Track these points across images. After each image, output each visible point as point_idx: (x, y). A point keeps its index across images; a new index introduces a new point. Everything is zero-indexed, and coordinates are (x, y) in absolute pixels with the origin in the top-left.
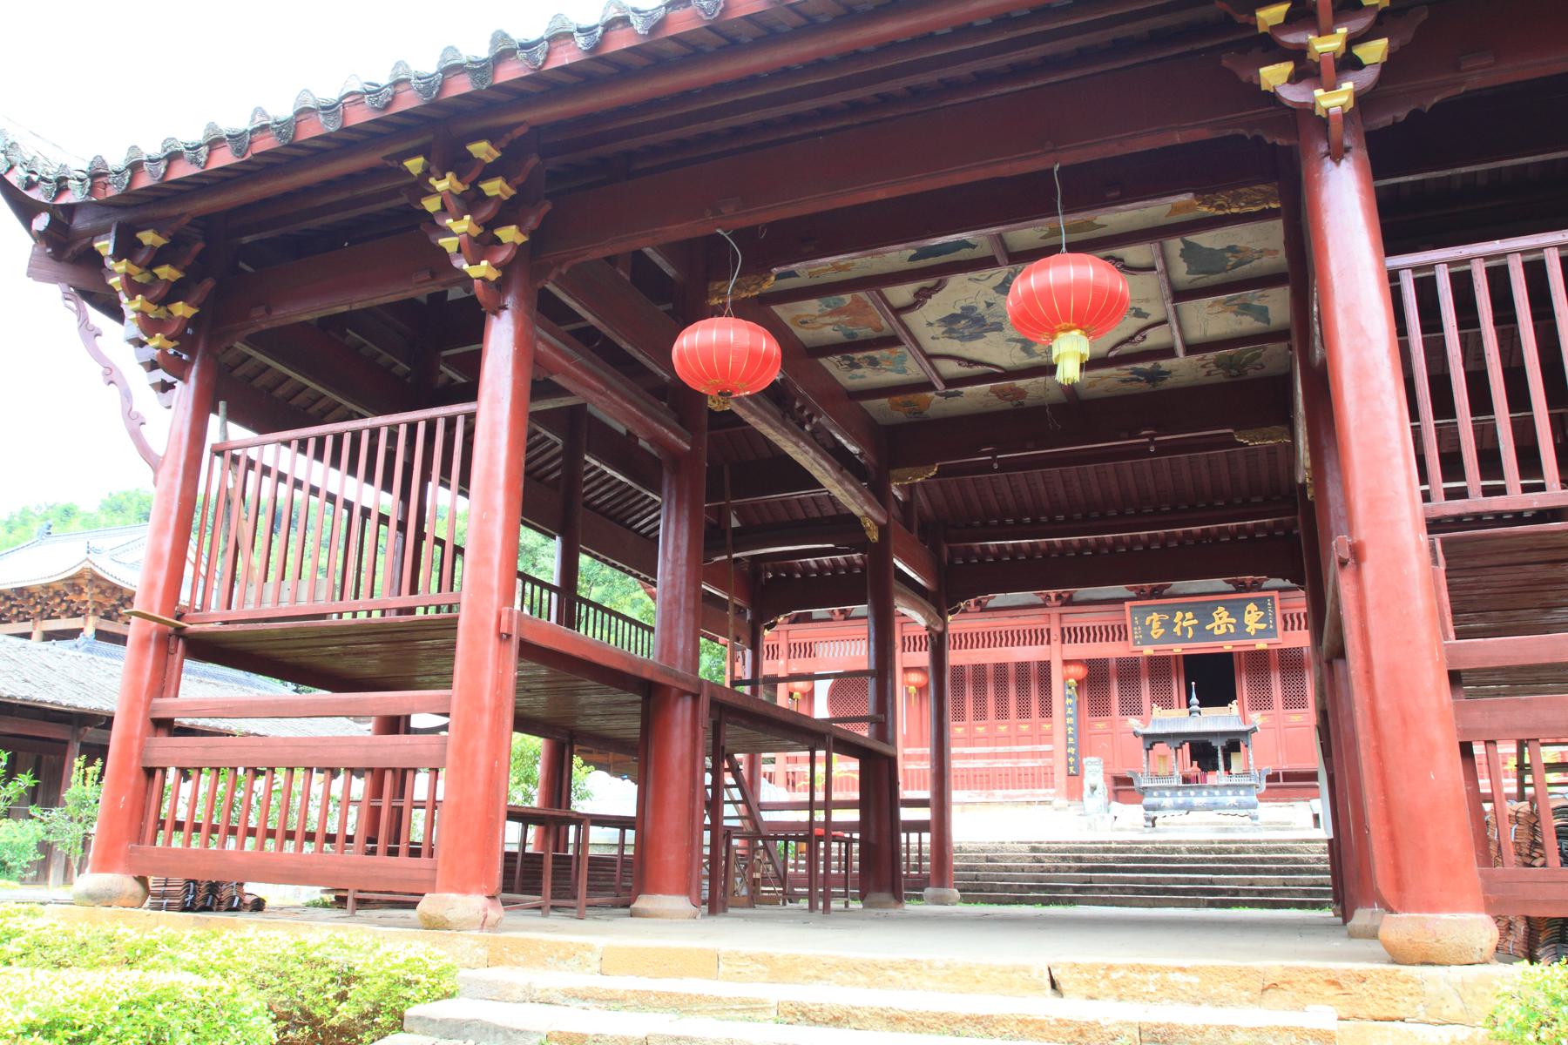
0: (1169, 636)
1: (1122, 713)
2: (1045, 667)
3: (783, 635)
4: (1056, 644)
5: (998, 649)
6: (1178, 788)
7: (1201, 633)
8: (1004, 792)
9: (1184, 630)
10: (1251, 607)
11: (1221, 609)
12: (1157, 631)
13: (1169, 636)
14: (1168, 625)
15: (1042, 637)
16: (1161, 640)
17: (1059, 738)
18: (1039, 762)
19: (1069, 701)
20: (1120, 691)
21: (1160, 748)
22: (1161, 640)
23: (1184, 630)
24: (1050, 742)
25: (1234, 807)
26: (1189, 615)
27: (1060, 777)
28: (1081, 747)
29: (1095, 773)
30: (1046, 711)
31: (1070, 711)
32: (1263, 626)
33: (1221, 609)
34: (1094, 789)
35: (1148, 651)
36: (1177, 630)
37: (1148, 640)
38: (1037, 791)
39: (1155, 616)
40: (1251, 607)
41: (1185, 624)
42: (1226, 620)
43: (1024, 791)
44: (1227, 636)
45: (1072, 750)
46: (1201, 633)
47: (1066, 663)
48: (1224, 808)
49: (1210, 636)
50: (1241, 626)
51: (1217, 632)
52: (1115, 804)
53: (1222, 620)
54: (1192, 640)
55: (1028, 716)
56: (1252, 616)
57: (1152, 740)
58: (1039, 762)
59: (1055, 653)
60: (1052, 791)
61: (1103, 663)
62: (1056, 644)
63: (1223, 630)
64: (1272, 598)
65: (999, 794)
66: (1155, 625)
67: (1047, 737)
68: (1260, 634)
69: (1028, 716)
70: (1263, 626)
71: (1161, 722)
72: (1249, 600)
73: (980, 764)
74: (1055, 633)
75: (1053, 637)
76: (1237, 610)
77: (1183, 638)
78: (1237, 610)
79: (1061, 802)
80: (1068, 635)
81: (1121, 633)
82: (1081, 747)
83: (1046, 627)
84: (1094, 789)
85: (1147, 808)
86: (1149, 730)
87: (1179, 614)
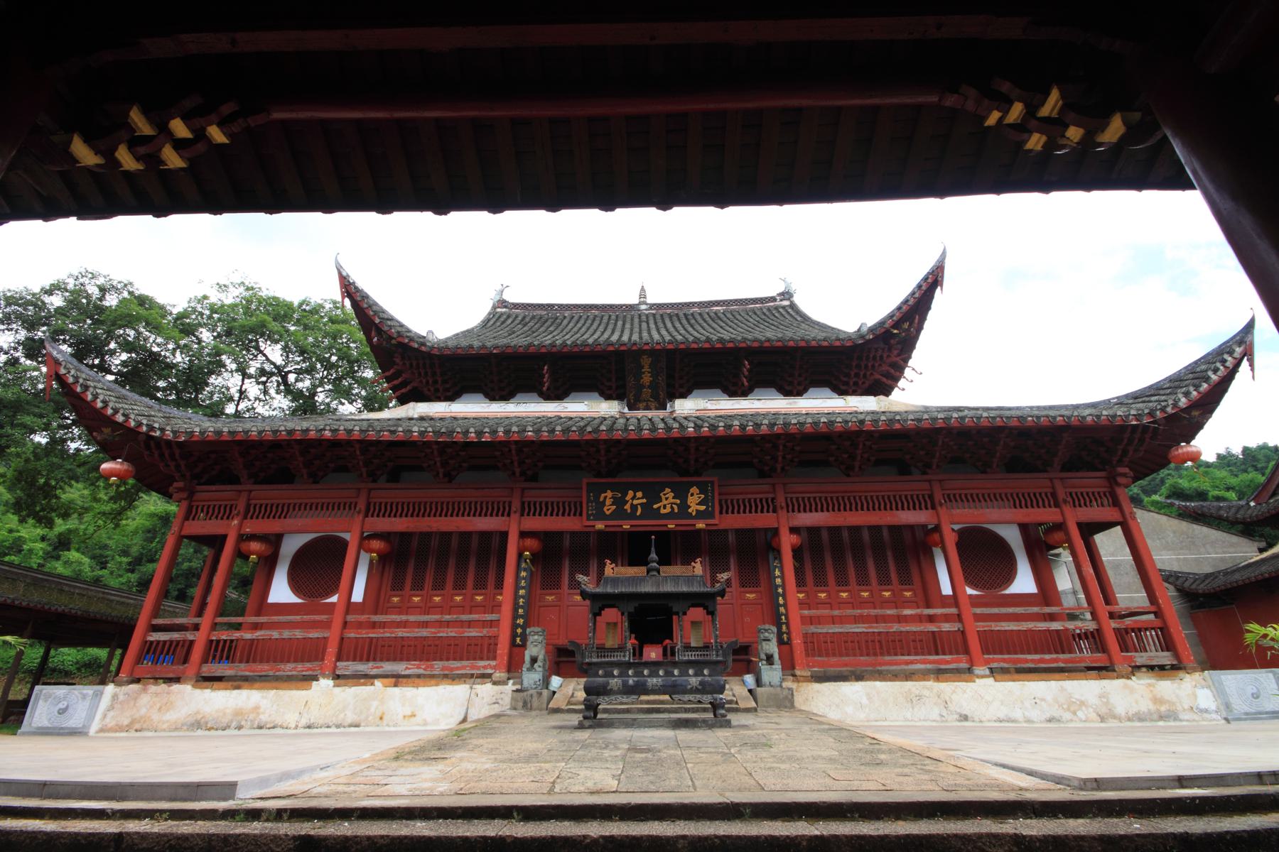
0: (620, 514)
1: (571, 587)
2: (504, 535)
3: (245, 495)
4: (515, 517)
5: (460, 518)
6: (629, 665)
7: (649, 511)
8: (446, 663)
9: (634, 507)
10: (694, 490)
11: (668, 490)
12: (609, 508)
13: (620, 514)
14: (619, 502)
15: (502, 510)
16: (613, 516)
17: (507, 610)
18: (485, 632)
19: (523, 574)
20: (571, 567)
21: (611, 614)
22: (613, 516)
23: (634, 507)
24: (499, 612)
25: (695, 691)
26: (639, 494)
27: (503, 648)
28: (529, 615)
29: (536, 647)
30: (499, 585)
31: (523, 583)
32: (703, 508)
33: (668, 490)
34: (534, 660)
35: (600, 526)
36: (627, 507)
37: (601, 516)
38: (482, 663)
39: (609, 494)
40: (694, 490)
41: (635, 502)
42: (671, 500)
43: (465, 663)
44: (671, 515)
45: (520, 621)
46: (649, 511)
47: (523, 535)
48: (685, 692)
49: (657, 514)
50: (684, 506)
51: (663, 511)
52: (556, 681)
53: (668, 502)
54: (641, 517)
55: (485, 587)
56: (694, 501)
57: (600, 602)
58: (485, 632)
59: (513, 526)
60: (493, 663)
61: (559, 534)
62: (515, 517)
63: (668, 510)
64: (712, 483)
65: (438, 665)
66: (608, 502)
67: (496, 607)
68: (700, 515)
69: (485, 587)
70: (703, 508)
71: (615, 581)
72: (692, 485)
73: (424, 633)
74: (516, 505)
75: (514, 509)
76: (681, 493)
77: (632, 516)
78: (681, 493)
79: (498, 675)
80: (527, 509)
81: (577, 511)
82: (529, 615)
83: (508, 499)
84: (534, 660)
85: (588, 690)
86: (599, 590)
87: (631, 493)
